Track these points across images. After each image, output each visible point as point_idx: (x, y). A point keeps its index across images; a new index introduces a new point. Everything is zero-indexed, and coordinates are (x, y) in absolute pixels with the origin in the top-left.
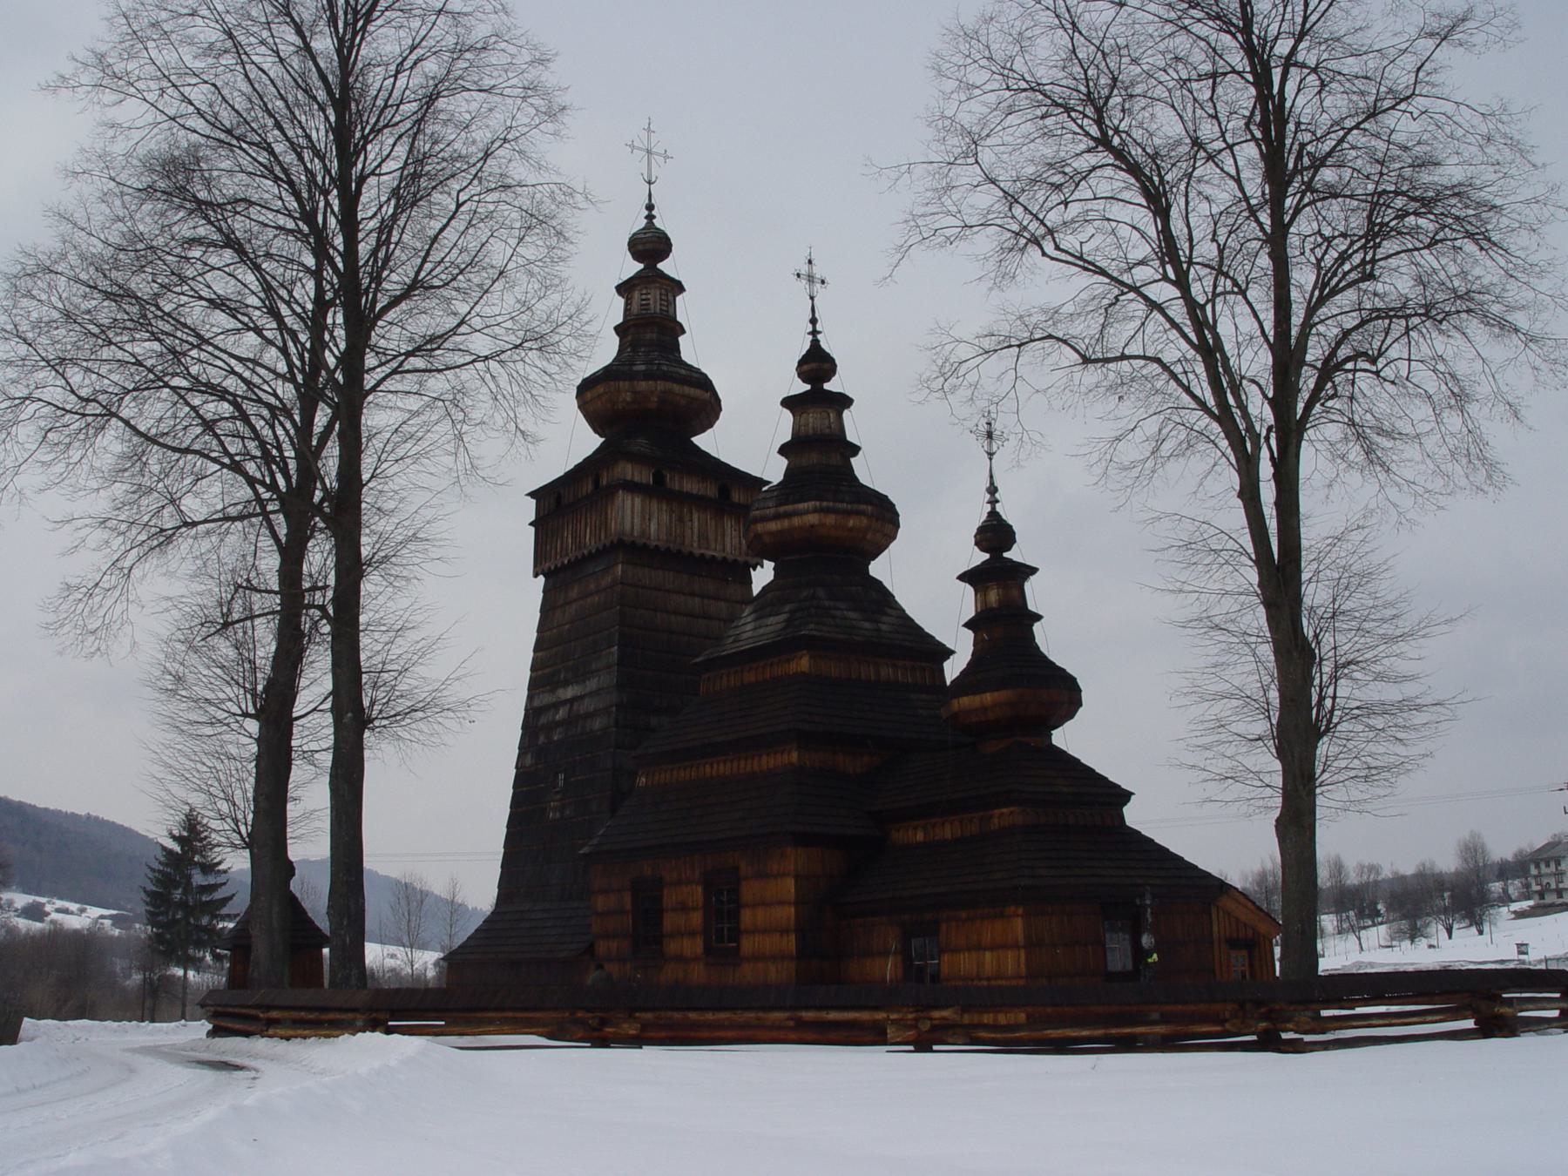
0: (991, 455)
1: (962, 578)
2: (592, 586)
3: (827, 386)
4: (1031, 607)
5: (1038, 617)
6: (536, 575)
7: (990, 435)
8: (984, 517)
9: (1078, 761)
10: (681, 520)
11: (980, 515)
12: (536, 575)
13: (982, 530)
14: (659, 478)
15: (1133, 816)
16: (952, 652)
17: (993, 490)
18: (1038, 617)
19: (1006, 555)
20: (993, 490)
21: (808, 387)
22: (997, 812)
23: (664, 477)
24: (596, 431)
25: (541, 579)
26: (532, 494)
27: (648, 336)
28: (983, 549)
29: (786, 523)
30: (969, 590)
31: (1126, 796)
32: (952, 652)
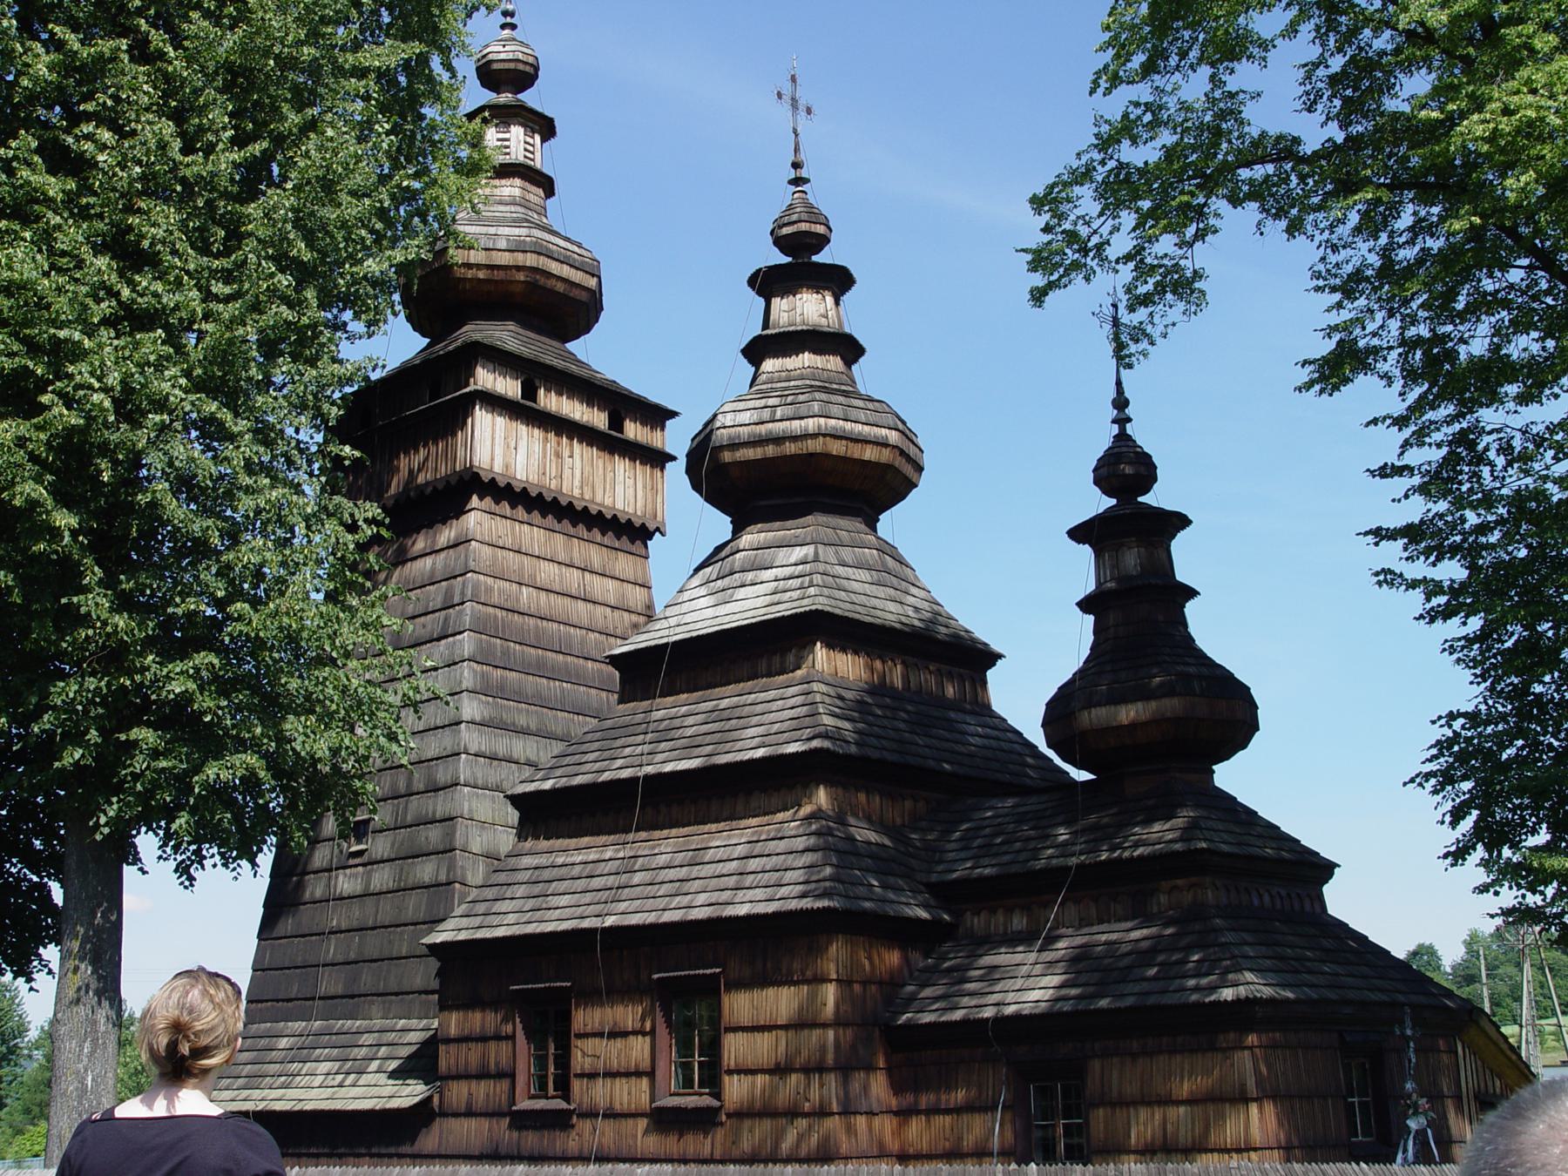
1: (1078, 534)
3: (815, 258)
4: (1180, 576)
5: (1191, 593)
9: (1253, 813)
10: (558, 455)
11: (1102, 438)
15: (1340, 900)
16: (1000, 656)
17: (1121, 403)
18: (1191, 593)
19: (1140, 499)
20: (1121, 403)
22: (1165, 885)
27: (507, 191)
28: (1107, 492)
29: (771, 451)
30: (1085, 554)
31: (1326, 869)
32: (1000, 656)
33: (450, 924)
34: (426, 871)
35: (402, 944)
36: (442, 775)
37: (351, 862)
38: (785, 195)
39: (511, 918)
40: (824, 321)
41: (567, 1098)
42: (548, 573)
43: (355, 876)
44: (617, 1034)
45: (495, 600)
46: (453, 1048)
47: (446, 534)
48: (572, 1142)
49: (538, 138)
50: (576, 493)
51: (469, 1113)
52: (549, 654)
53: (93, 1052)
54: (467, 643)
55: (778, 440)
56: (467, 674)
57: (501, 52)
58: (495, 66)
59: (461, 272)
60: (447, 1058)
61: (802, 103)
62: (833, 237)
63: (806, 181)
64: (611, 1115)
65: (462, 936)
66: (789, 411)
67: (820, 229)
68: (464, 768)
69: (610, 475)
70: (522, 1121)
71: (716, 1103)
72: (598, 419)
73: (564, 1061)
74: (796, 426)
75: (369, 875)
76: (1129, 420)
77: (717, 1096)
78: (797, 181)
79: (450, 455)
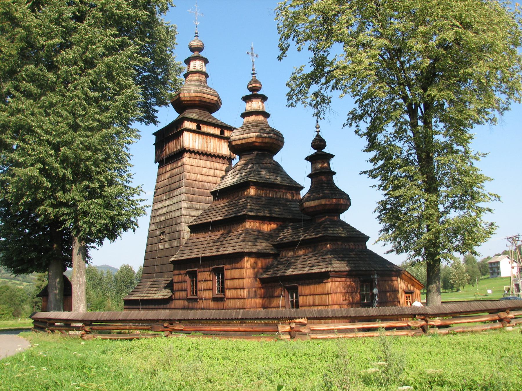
1: (307, 159)
2: (175, 166)
4: (332, 169)
5: (334, 173)
6: (155, 163)
8: (315, 137)
11: (313, 136)
12: (155, 163)
13: (314, 141)
14: (199, 127)
18: (334, 173)
23: (200, 127)
24: (177, 112)
25: (158, 164)
26: (154, 134)
29: (243, 141)
30: (309, 164)
33: (175, 256)
34: (175, 243)
35: (165, 260)
36: (178, 221)
37: (162, 241)
38: (251, 77)
39: (186, 255)
40: (259, 108)
41: (197, 296)
42: (205, 171)
43: (162, 245)
44: (206, 281)
45: (191, 178)
46: (176, 284)
47: (180, 163)
48: (198, 305)
49: (203, 63)
50: (212, 151)
51: (179, 299)
52: (205, 190)
53: (80, 287)
54: (183, 189)
55: (245, 139)
56: (183, 197)
57: (194, 43)
58: (193, 47)
59: (183, 99)
61: (255, 55)
62: (262, 87)
63: (255, 74)
64: (205, 299)
65: (176, 259)
66: (247, 131)
67: (258, 85)
68: (183, 219)
69: (221, 146)
70: (189, 300)
71: (223, 296)
72: (217, 132)
73: (196, 286)
74: (249, 135)
75: (164, 244)
76: (319, 131)
77: (224, 295)
78: (253, 74)
79: (179, 144)
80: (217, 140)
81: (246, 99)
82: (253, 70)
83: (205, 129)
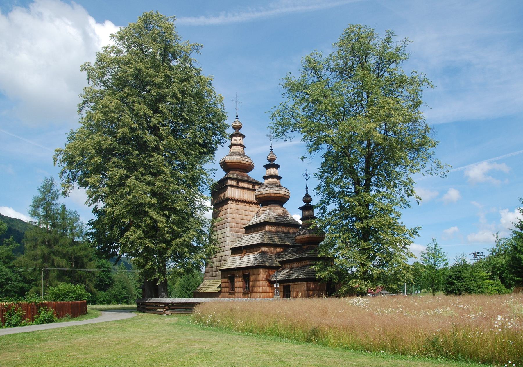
0: (307, 180)
7: (307, 175)
21: (270, 162)
30: (301, 212)
57: (237, 124)
60: (222, 286)
72: (250, 186)
80: (250, 192)
81: (267, 167)
82: (271, 147)
83: (242, 184)
